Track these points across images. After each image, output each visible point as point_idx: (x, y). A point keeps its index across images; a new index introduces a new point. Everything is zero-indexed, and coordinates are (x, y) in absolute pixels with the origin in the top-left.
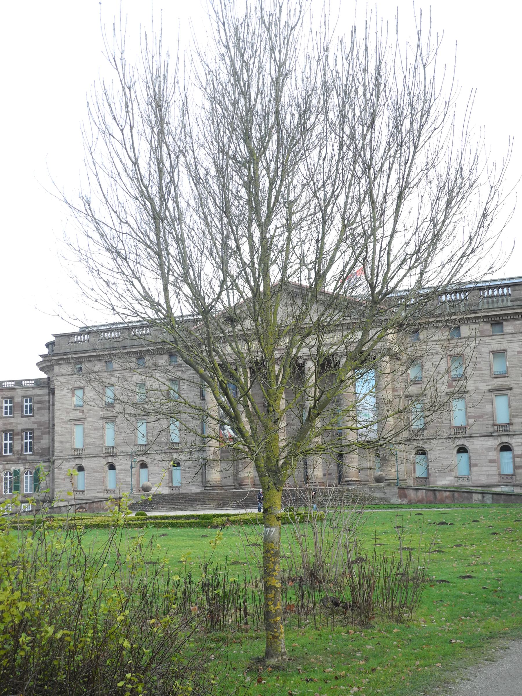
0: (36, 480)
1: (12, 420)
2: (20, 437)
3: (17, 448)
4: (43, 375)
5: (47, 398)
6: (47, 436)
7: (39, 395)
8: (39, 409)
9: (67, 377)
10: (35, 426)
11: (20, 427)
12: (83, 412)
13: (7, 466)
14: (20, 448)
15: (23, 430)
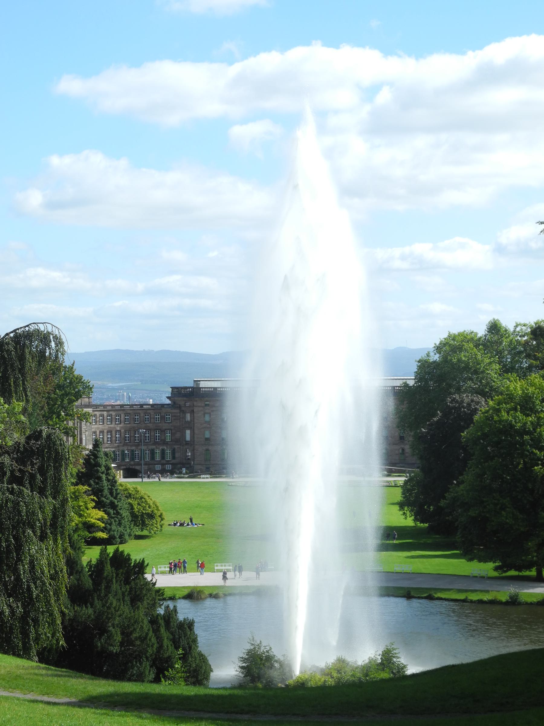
0: (173, 452)
1: (160, 424)
2: (164, 433)
3: (163, 438)
4: (168, 402)
5: (179, 414)
6: (179, 432)
7: (174, 413)
8: (174, 419)
9: (201, 408)
10: (172, 428)
11: (164, 428)
12: (210, 425)
13: (158, 447)
14: (164, 438)
15: (166, 429)
